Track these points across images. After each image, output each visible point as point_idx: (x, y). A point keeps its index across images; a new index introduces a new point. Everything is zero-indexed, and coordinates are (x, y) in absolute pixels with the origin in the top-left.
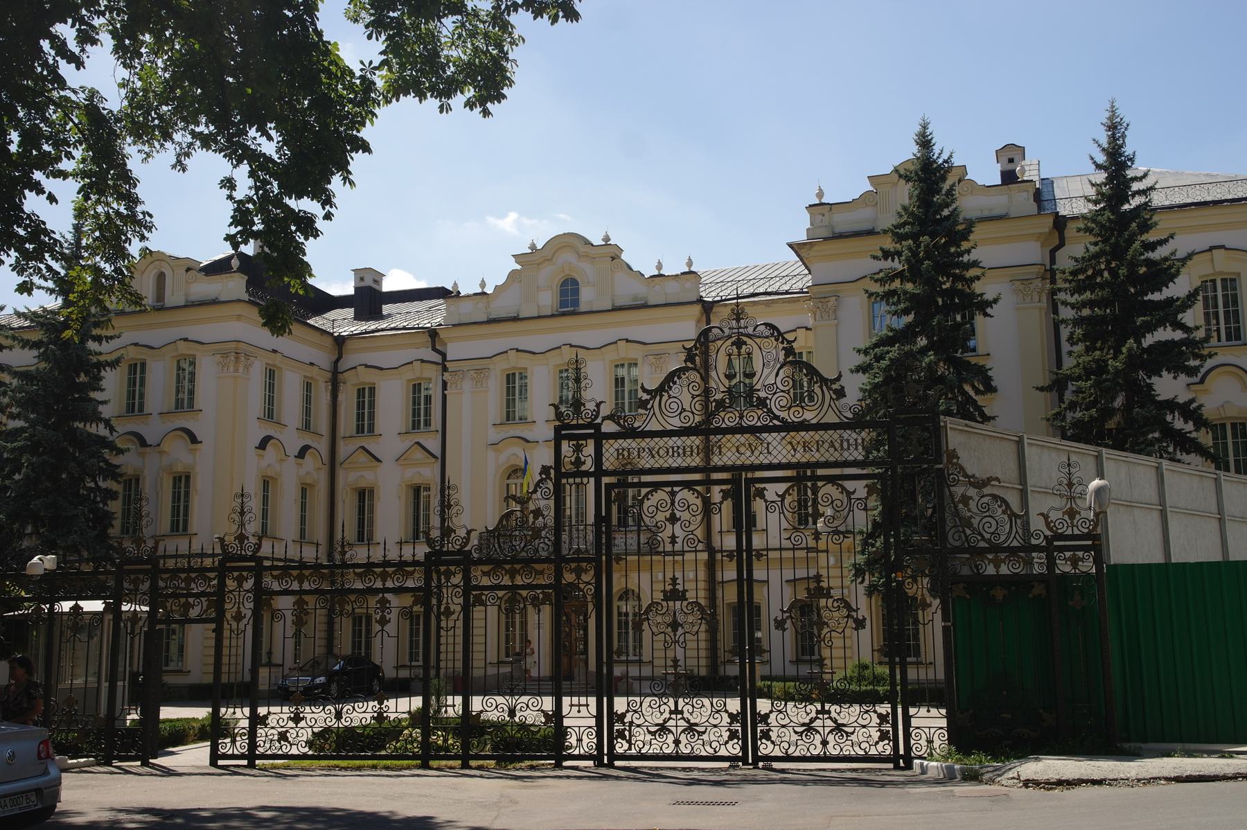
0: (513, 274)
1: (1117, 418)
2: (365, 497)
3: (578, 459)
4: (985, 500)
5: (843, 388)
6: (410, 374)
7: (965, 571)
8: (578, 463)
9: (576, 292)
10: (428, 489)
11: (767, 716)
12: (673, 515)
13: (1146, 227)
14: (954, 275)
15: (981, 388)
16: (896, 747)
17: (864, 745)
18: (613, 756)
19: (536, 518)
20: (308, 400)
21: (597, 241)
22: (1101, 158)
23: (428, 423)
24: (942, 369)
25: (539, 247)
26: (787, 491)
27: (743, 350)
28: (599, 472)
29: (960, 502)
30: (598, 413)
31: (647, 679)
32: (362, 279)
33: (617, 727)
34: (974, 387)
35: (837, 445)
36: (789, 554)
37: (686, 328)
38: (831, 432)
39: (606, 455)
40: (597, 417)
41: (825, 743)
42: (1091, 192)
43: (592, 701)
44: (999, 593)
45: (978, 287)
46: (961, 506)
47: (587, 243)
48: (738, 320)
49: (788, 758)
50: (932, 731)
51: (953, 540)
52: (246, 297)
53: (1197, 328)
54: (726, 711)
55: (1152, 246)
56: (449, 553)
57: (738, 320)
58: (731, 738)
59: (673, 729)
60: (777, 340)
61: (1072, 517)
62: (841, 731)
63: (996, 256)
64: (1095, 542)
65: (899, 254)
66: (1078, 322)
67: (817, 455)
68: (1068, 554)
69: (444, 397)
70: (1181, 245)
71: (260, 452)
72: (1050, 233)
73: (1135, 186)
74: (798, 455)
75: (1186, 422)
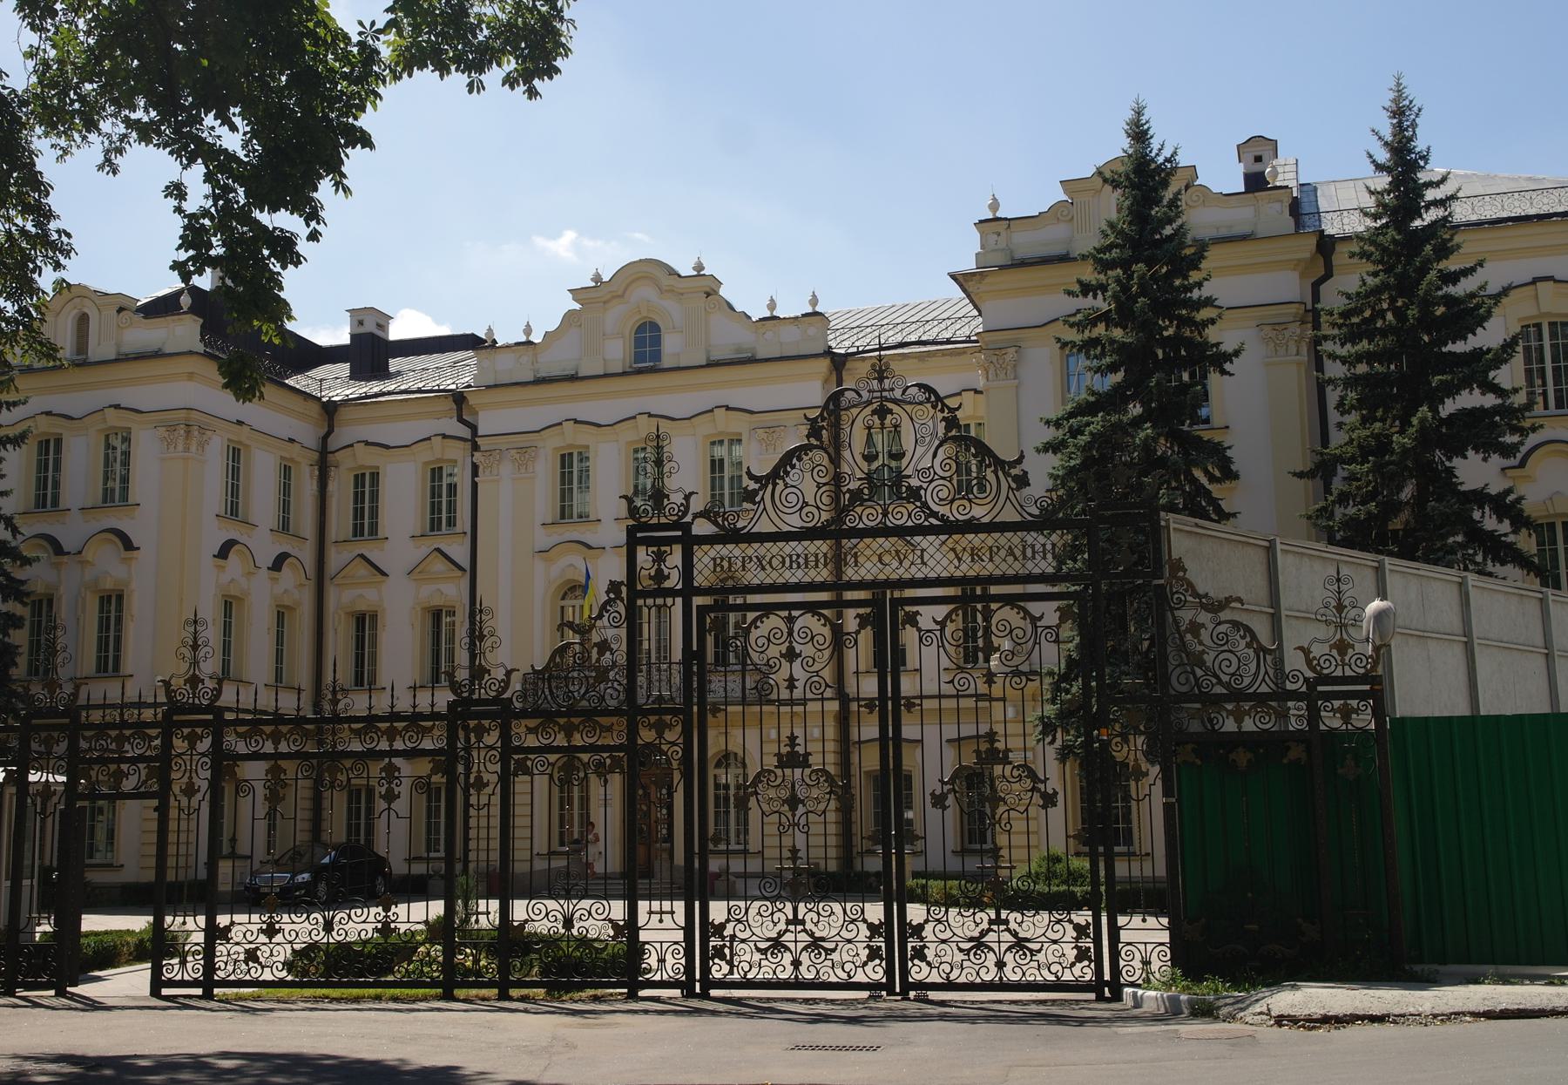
0: (570, 315)
1: (1405, 515)
2: (364, 624)
3: (659, 571)
4: (1222, 628)
5: (1026, 473)
6: (426, 454)
7: (1195, 727)
8: (660, 576)
9: (657, 341)
10: (452, 613)
11: (921, 927)
12: (791, 650)
13: (1444, 251)
14: (1180, 317)
15: (1217, 474)
16: (1099, 971)
17: (1054, 968)
18: (708, 983)
19: (601, 653)
20: (286, 490)
21: (686, 270)
22: (1383, 156)
23: (451, 522)
24: (1162, 447)
25: (606, 278)
26: (948, 616)
27: (887, 422)
28: (689, 590)
29: (1187, 631)
30: (687, 508)
31: (754, 876)
32: (361, 323)
33: (714, 942)
34: (1206, 472)
35: (1018, 553)
36: (952, 703)
37: (811, 390)
38: (1009, 535)
39: (698, 566)
40: (685, 513)
41: (1000, 965)
42: (1369, 202)
43: (679, 906)
44: (1242, 758)
45: (1212, 334)
46: (1189, 637)
47: (673, 273)
48: (881, 379)
49: (950, 986)
50: (1150, 947)
51: (1178, 685)
52: (200, 348)
53: (1516, 391)
54: (865, 921)
55: (1453, 278)
56: (480, 702)
57: (881, 379)
58: (871, 958)
59: (791, 946)
60: (934, 407)
61: (1342, 653)
62: (1022, 948)
63: (1240, 293)
64: (1375, 686)
65: (1103, 288)
66: (1351, 382)
67: (990, 567)
68: (1337, 703)
69: (475, 486)
70: (1493, 276)
71: (220, 562)
72: (1312, 259)
73: (1430, 194)
74: (964, 567)
75: (1500, 521)
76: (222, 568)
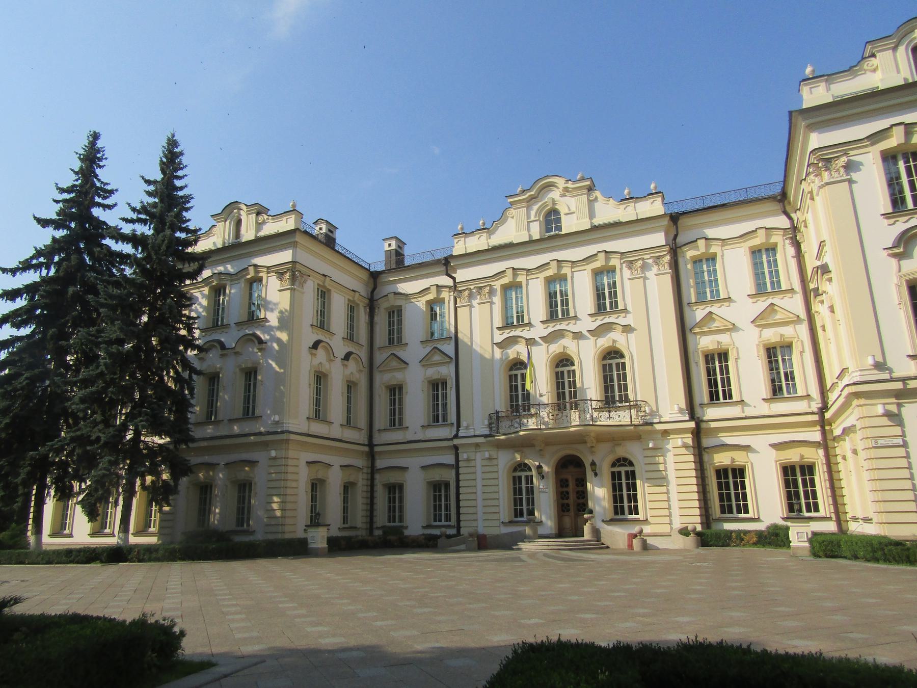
2: (396, 391)
9: (559, 220)
10: (444, 384)
76: (313, 355)
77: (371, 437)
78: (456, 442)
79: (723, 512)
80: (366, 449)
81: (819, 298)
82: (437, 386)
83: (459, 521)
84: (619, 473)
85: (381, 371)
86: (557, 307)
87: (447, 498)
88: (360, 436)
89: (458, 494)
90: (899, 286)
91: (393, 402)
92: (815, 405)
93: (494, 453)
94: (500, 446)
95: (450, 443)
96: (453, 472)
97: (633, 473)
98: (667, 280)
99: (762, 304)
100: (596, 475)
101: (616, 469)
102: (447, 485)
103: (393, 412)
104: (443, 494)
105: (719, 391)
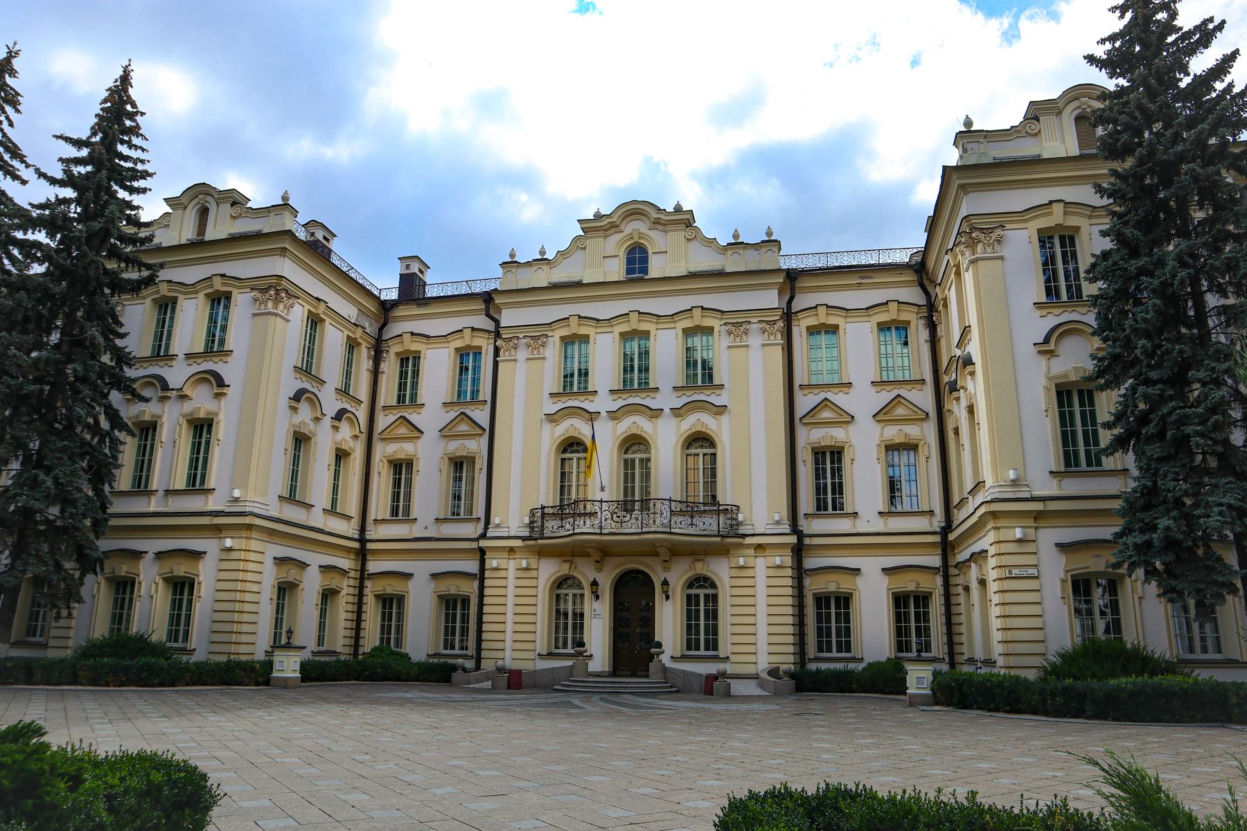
0: (577, 238)
2: (402, 469)
9: (645, 260)
10: (472, 460)
20: (349, 363)
23: (475, 393)
69: (496, 365)
71: (294, 404)
76: (294, 409)
77: (363, 529)
78: (483, 543)
79: (820, 650)
80: (356, 545)
81: (955, 394)
82: (459, 464)
83: (479, 649)
84: (697, 596)
85: (383, 439)
86: (635, 373)
87: (465, 619)
88: (349, 528)
89: (480, 614)
90: (1047, 389)
91: (397, 483)
92: (938, 522)
93: (534, 564)
94: (542, 553)
95: (474, 545)
96: (476, 584)
97: (715, 597)
98: (777, 354)
99: (886, 396)
100: (667, 598)
101: (693, 591)
102: (465, 601)
103: (396, 497)
104: (460, 612)
105: (831, 497)
